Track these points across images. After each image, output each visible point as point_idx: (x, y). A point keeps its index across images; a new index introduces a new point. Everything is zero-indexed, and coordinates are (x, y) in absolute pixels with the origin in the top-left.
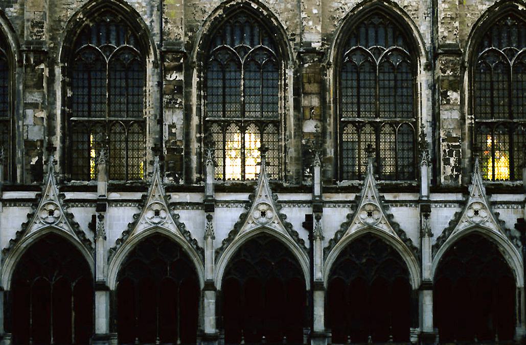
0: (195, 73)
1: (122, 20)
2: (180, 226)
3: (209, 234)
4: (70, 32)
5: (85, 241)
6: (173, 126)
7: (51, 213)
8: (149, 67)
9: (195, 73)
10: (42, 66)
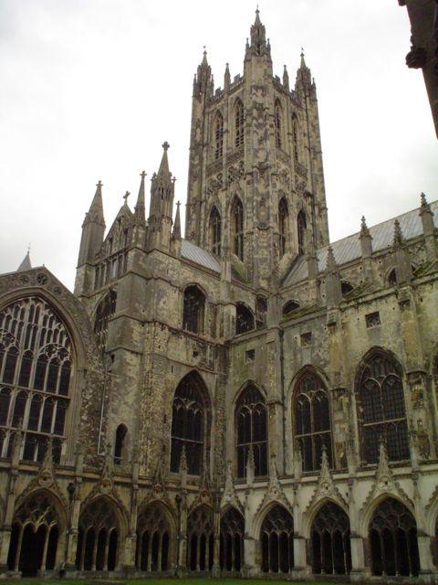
0: (433, 382)
1: (387, 360)
2: (401, 491)
3: (417, 495)
4: (359, 373)
5: (346, 504)
6: (420, 421)
7: (327, 488)
8: (405, 385)
9: (433, 382)
10: (342, 397)
